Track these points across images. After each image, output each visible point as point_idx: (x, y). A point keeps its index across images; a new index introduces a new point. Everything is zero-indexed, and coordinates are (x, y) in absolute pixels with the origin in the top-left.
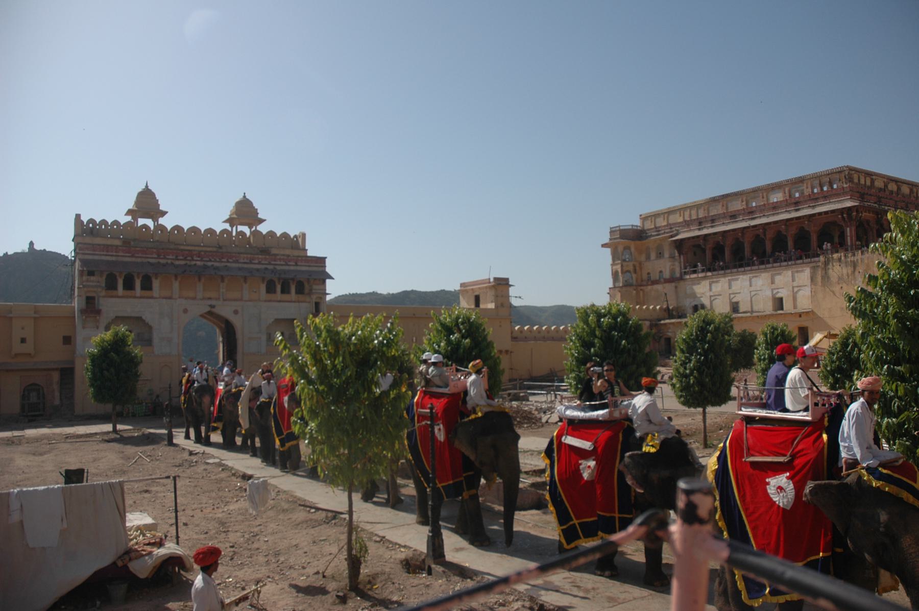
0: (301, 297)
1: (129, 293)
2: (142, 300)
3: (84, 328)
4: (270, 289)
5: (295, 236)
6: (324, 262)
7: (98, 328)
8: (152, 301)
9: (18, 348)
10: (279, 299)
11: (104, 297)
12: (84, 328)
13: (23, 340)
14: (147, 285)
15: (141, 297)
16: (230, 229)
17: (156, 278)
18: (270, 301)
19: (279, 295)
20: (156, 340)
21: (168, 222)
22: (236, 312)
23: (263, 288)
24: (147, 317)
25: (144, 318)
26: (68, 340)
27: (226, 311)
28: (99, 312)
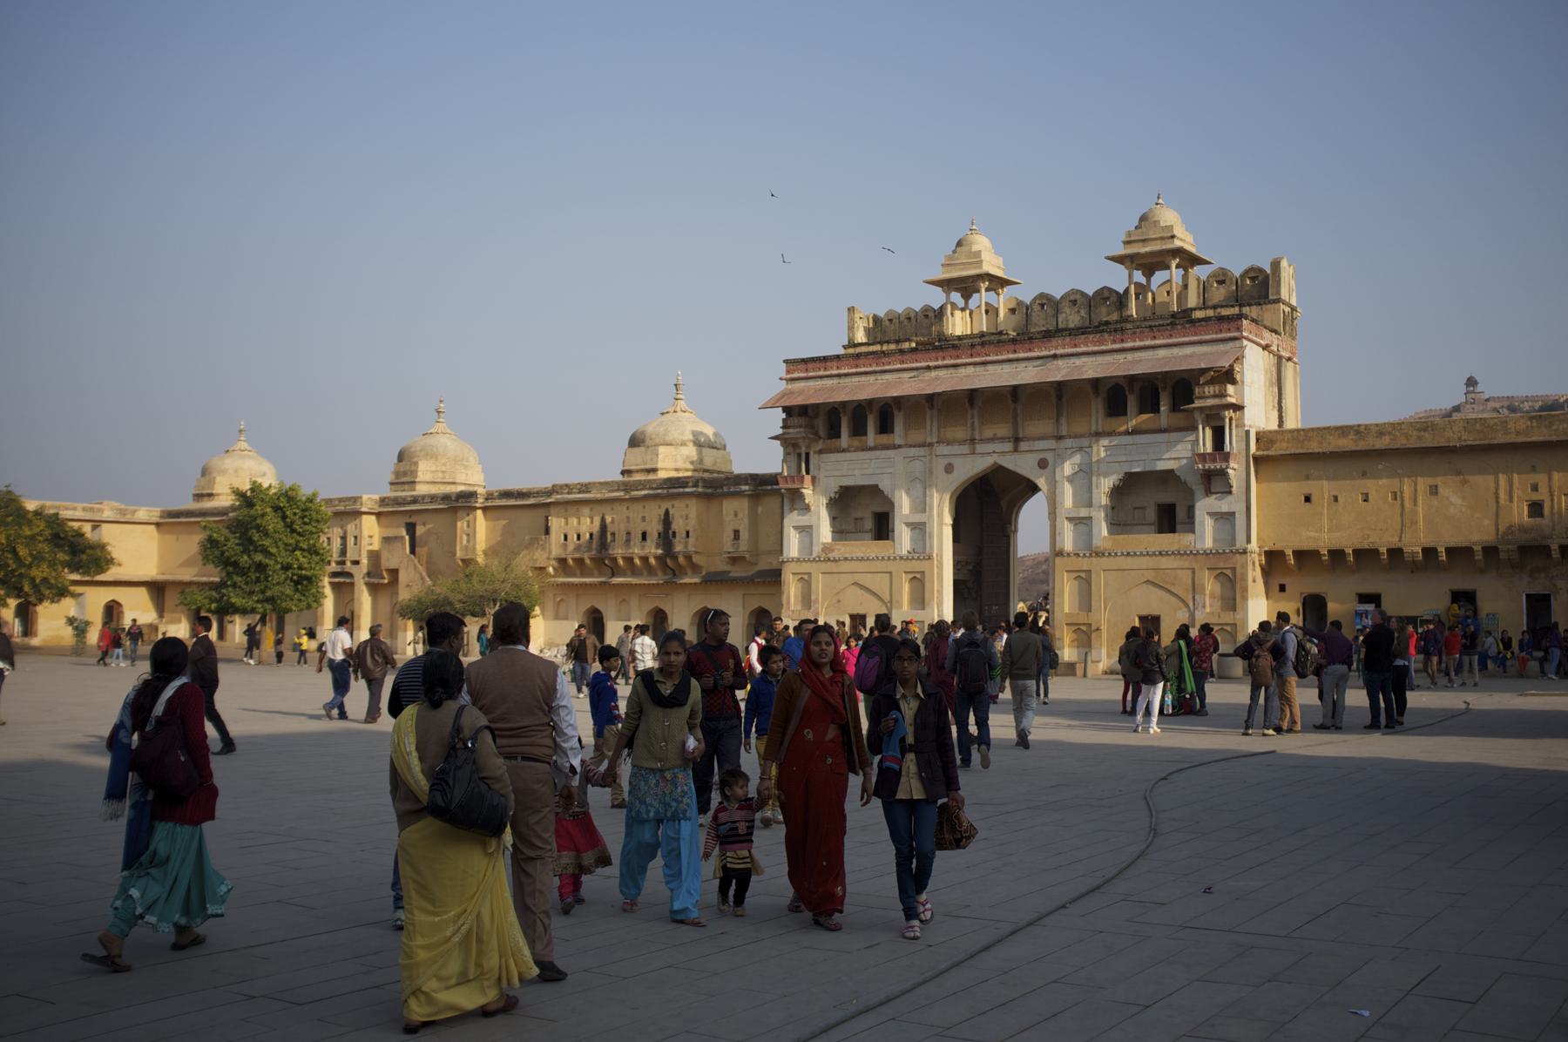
0: (1178, 419)
1: (856, 442)
2: (878, 453)
8: (891, 453)
11: (820, 452)
12: (792, 510)
14: (885, 427)
17: (899, 409)
21: (1026, 293)
22: (1043, 464)
23: (1097, 406)
24: (884, 485)
25: (881, 486)
27: (1023, 464)
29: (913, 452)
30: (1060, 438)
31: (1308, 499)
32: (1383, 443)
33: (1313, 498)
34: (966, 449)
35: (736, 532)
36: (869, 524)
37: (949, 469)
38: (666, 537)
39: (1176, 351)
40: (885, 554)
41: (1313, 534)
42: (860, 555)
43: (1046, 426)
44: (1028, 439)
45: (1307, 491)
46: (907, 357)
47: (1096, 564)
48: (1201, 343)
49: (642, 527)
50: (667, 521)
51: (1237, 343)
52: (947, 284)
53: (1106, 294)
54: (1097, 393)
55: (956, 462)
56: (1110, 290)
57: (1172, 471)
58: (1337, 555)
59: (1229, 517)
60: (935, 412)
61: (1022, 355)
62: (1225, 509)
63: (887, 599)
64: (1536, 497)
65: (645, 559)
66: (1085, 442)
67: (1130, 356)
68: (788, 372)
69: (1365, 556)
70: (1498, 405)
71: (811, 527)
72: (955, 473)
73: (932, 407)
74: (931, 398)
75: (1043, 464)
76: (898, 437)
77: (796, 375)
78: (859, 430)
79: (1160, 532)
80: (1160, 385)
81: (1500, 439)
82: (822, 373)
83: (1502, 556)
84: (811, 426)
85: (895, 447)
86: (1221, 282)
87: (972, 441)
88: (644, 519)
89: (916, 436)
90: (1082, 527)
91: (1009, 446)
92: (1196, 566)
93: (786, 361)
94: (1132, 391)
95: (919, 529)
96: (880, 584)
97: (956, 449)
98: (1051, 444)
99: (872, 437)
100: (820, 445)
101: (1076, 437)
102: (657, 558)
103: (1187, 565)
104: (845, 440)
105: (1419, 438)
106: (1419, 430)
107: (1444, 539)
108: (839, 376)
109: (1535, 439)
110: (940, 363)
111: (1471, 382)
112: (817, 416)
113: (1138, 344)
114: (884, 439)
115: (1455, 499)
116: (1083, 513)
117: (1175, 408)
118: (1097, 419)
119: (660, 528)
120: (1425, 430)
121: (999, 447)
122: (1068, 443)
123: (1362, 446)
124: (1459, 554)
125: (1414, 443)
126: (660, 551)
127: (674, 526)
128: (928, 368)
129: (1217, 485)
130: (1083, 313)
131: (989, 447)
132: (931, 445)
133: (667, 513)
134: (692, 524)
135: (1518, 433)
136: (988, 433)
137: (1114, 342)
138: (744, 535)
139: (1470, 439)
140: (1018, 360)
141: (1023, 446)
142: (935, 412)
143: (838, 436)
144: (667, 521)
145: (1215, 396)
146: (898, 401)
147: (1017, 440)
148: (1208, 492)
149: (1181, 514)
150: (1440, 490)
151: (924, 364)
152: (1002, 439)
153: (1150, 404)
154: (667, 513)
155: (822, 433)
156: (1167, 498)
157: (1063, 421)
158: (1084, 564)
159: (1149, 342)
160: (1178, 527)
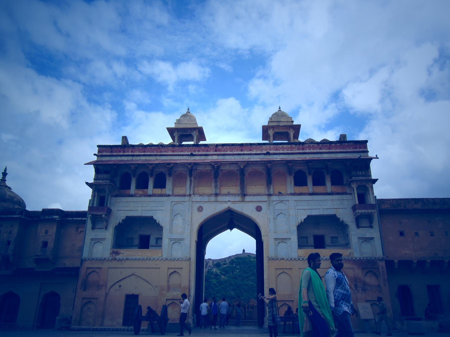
1: (140, 192)
3: (93, 228)
4: (300, 181)
6: (366, 147)
7: (106, 228)
10: (311, 191)
11: (116, 196)
17: (170, 175)
18: (300, 194)
19: (310, 187)
20: (165, 242)
22: (259, 209)
23: (290, 180)
25: (155, 217)
27: (246, 209)
28: (109, 211)
30: (270, 195)
31: (402, 234)
34: (213, 198)
35: (45, 244)
36: (137, 241)
37: (200, 209)
40: (156, 257)
41: (408, 252)
42: (138, 257)
43: (261, 188)
44: (250, 195)
54: (290, 174)
55: (205, 206)
57: (336, 215)
58: (421, 263)
60: (193, 179)
61: (246, 152)
62: (368, 236)
68: (99, 151)
71: (104, 239)
72: (204, 211)
73: (191, 175)
75: (259, 209)
76: (168, 190)
77: (105, 154)
82: (121, 154)
84: (112, 181)
87: (216, 195)
89: (179, 190)
90: (282, 244)
91: (238, 198)
93: (99, 146)
94: (310, 174)
97: (206, 198)
98: (265, 198)
99: (151, 189)
108: (133, 156)
110: (197, 153)
113: (312, 151)
114: (158, 191)
117: (333, 184)
118: (290, 187)
121: (232, 199)
122: (274, 198)
128: (192, 155)
131: (227, 198)
136: (224, 190)
137: (299, 149)
138: (51, 245)
140: (244, 154)
141: (247, 198)
142: (193, 179)
147: (244, 195)
149: (328, 241)
152: (234, 195)
153: (319, 181)
155: (118, 185)
156: (319, 232)
157: (272, 187)
159: (318, 151)
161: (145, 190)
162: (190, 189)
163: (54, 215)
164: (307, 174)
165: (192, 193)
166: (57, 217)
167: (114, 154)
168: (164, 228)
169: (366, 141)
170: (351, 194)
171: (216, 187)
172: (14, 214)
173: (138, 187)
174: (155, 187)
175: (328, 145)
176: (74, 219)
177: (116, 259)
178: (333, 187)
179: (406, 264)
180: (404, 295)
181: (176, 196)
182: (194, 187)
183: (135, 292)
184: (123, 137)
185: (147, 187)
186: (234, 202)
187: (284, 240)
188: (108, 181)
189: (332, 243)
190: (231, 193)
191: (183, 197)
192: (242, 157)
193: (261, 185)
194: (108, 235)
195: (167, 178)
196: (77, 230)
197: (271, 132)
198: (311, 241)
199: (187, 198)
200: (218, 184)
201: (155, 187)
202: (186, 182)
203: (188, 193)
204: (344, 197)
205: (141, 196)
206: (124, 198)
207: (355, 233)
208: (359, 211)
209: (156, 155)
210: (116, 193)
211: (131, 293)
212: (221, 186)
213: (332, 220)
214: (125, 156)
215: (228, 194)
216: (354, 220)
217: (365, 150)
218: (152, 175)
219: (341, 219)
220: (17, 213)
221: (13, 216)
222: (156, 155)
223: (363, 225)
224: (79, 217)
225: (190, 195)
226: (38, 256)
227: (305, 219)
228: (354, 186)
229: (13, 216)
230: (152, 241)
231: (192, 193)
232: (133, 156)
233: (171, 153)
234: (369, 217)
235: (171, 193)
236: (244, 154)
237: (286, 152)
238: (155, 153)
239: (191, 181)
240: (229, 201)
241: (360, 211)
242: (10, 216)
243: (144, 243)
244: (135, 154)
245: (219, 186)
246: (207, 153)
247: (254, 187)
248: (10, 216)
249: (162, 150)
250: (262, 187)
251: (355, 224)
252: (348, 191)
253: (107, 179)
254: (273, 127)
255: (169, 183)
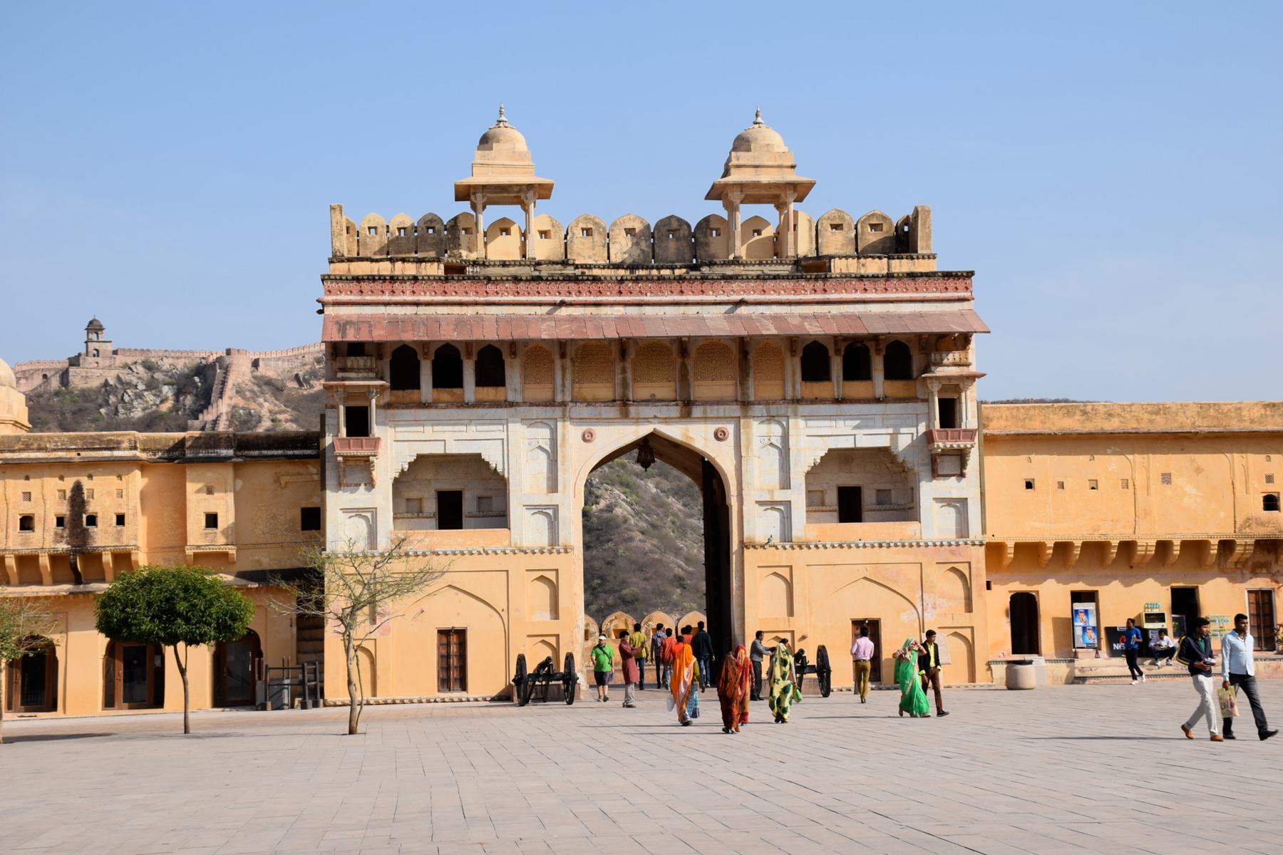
0: (897, 387)
1: (445, 395)
5: (906, 221)
9: (197, 536)
11: (389, 406)
13: (212, 520)
15: (479, 404)
16: (724, 214)
17: (514, 354)
19: (836, 384)
23: (793, 366)
24: (493, 456)
25: (485, 457)
26: (313, 519)
29: (536, 412)
31: (1029, 485)
32: (1113, 425)
33: (1036, 484)
34: (613, 411)
36: (431, 506)
38: (77, 519)
39: (891, 308)
43: (726, 388)
45: (1029, 477)
46: (522, 286)
47: (798, 558)
48: (923, 301)
49: (27, 508)
50: (77, 499)
51: (965, 305)
52: (463, 193)
53: (675, 225)
54: (793, 352)
56: (679, 220)
58: (1063, 548)
59: (960, 505)
60: (568, 362)
63: (500, 604)
64: (1271, 489)
65: (27, 562)
66: (782, 409)
67: (835, 309)
69: (1096, 549)
70: (129, 360)
73: (563, 356)
74: (562, 346)
77: (343, 298)
78: (448, 375)
79: (841, 521)
80: (871, 346)
81: (1235, 426)
82: (386, 298)
83: (1239, 550)
85: (512, 405)
86: (836, 227)
88: (28, 496)
91: (674, 411)
92: (923, 560)
94: (837, 352)
95: (552, 515)
96: (493, 588)
99: (470, 389)
100: (387, 398)
101: (768, 403)
102: (55, 558)
103: (912, 559)
104: (426, 389)
105: (1151, 421)
106: (1151, 413)
107: (1179, 533)
108: (417, 304)
109: (1270, 428)
110: (573, 298)
111: (94, 327)
112: (380, 357)
113: (845, 296)
114: (489, 393)
115: (1189, 489)
116: (780, 495)
119: (64, 510)
120: (1157, 413)
123: (1089, 427)
124: (1195, 548)
125: (1144, 427)
126: (63, 547)
127: (92, 508)
129: (946, 465)
130: (643, 245)
132: (563, 404)
133: (78, 488)
134: (131, 506)
135: (1252, 421)
136: (643, 391)
139: (1204, 426)
140: (687, 304)
141: (697, 411)
142: (568, 362)
143: (416, 385)
144: (77, 499)
145: (955, 365)
146: (513, 345)
148: (935, 474)
149: (868, 498)
150: (1174, 479)
151: (558, 299)
153: (857, 368)
154: (78, 488)
156: (849, 480)
158: (783, 556)
159: (859, 296)
160: (865, 514)
161: (457, 391)
162: (563, 391)
163: (218, 447)
164: (831, 353)
165: (568, 398)
166: (231, 452)
167: (368, 298)
168: (512, 482)
169: (972, 273)
170: (926, 401)
171: (625, 385)
172: (118, 449)
173: (437, 384)
174: (480, 382)
175: (883, 281)
176: (265, 452)
177: (407, 555)
178: (889, 382)
179: (1029, 552)
180: (1024, 613)
181: (532, 404)
182: (573, 382)
183: (459, 625)
184: (332, 208)
185: (459, 383)
186: (666, 420)
187: (771, 504)
188: (371, 375)
189: (879, 503)
190: (659, 396)
191: (548, 409)
192: (682, 309)
193: (728, 379)
194: (381, 497)
195: (508, 360)
196: (277, 480)
197: (735, 196)
198: (832, 498)
199: (558, 411)
200: (629, 375)
201: (480, 382)
202: (552, 370)
203: (559, 399)
204: (910, 407)
205: (449, 405)
206: (407, 411)
207: (930, 491)
208: (940, 444)
209: (476, 304)
210: (387, 398)
211: (448, 626)
212: (635, 380)
213: (883, 454)
214: (396, 304)
215: (652, 401)
216: (928, 461)
217: (967, 294)
218: (469, 354)
219: (900, 460)
220: (126, 445)
221: (116, 453)
222: (476, 304)
223: (945, 472)
224: (277, 449)
225: (563, 404)
226: (198, 547)
227: (822, 458)
228: (935, 388)
229: (116, 453)
230: (468, 505)
231: (568, 398)
232: (417, 304)
233: (511, 298)
234: (961, 456)
235: (519, 399)
236: (687, 304)
237: (784, 297)
238: (471, 298)
239: (563, 369)
240: (655, 417)
241: (941, 445)
242: (107, 454)
243: (450, 513)
244: (422, 298)
245: (630, 381)
246: (599, 299)
247: (709, 382)
248: (107, 454)
249: (490, 287)
250: (730, 382)
251: (929, 468)
252: (920, 395)
253: (371, 370)
254: (741, 186)
255: (513, 374)
